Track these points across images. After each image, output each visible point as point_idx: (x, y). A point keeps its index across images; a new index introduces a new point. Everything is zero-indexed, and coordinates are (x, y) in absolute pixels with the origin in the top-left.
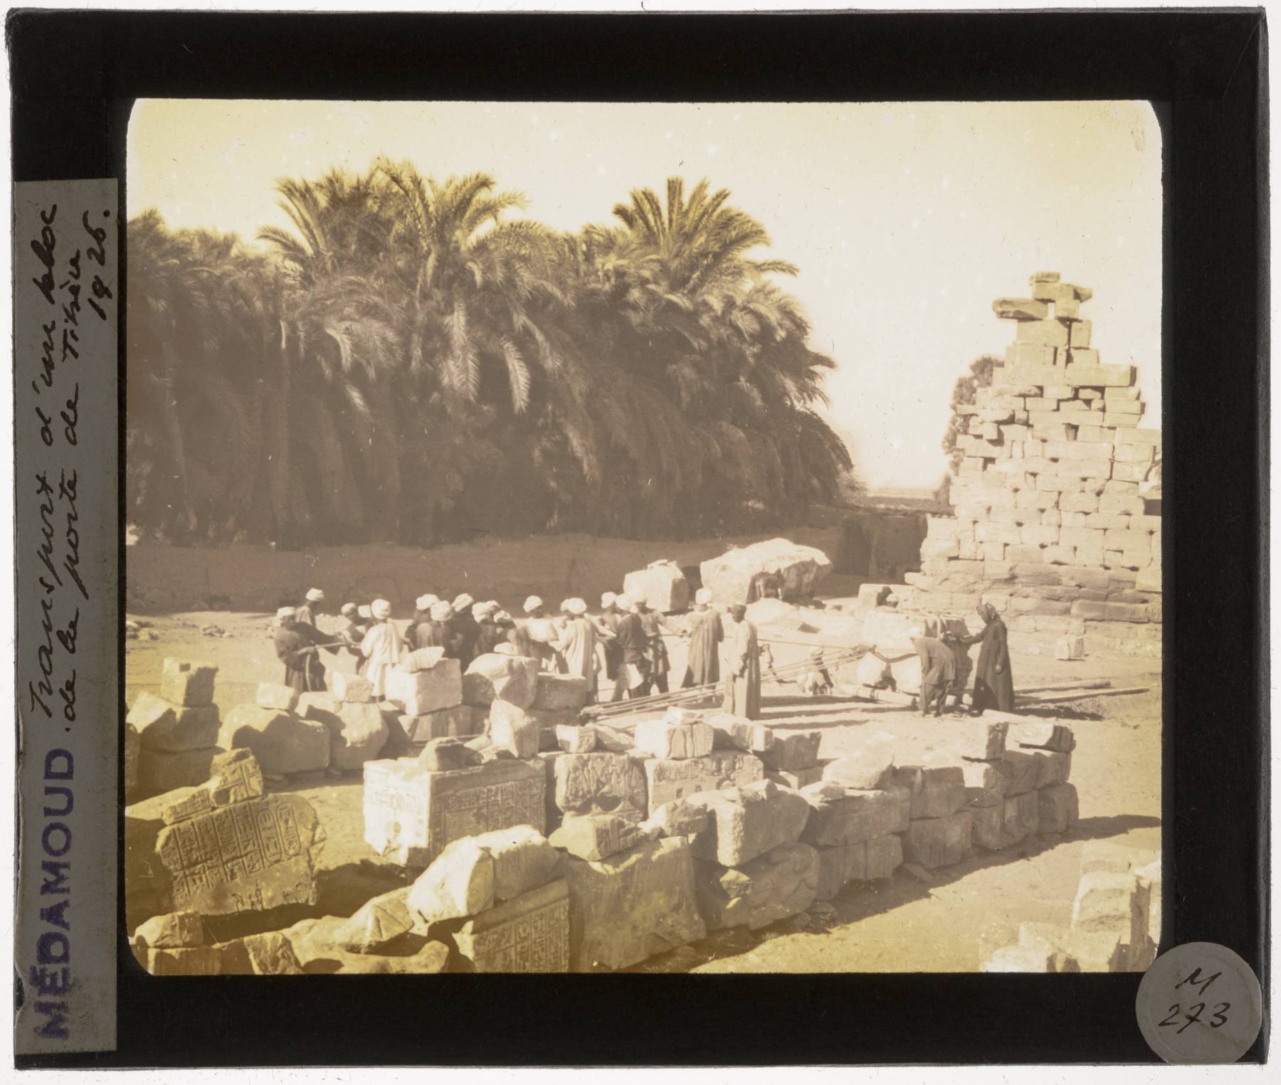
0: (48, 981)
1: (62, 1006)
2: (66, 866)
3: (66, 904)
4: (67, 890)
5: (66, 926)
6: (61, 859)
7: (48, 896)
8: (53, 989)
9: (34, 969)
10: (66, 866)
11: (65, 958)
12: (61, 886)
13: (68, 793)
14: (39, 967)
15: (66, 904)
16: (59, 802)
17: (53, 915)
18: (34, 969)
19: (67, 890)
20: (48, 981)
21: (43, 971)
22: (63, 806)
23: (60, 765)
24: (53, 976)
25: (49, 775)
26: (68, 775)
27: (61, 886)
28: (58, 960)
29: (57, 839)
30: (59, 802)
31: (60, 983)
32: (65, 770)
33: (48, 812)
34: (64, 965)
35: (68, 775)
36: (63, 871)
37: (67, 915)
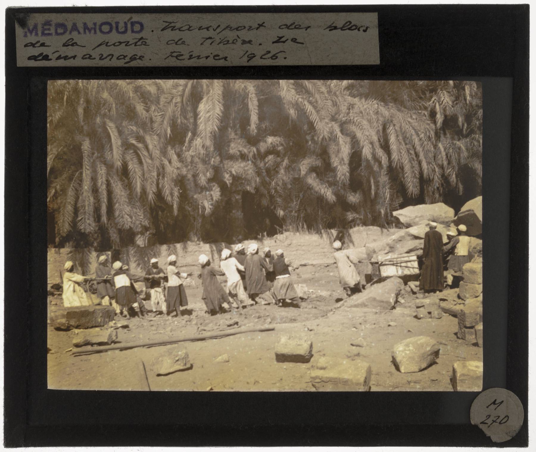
0: (45, 27)
1: (37, 34)
2: (95, 33)
3: (79, 33)
4: (85, 33)
5: (70, 33)
6: (98, 31)
7: (82, 25)
8: (44, 30)
9: (51, 21)
10: (95, 33)
11: (57, 34)
12: (87, 31)
13: (125, 32)
14: (53, 23)
15: (79, 33)
16: (121, 29)
17: (75, 28)
18: (51, 21)
19: (85, 33)
20: (45, 27)
21: (50, 25)
22: (120, 30)
23: (137, 27)
24: (49, 29)
25: (133, 24)
26: (133, 31)
27: (87, 31)
28: (56, 30)
29: (106, 28)
30: (121, 29)
31: (46, 32)
32: (135, 30)
33: (117, 23)
34: (54, 34)
35: (133, 31)
36: (93, 31)
37: (75, 33)
